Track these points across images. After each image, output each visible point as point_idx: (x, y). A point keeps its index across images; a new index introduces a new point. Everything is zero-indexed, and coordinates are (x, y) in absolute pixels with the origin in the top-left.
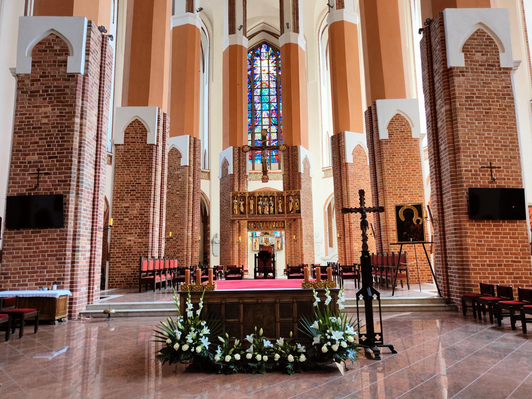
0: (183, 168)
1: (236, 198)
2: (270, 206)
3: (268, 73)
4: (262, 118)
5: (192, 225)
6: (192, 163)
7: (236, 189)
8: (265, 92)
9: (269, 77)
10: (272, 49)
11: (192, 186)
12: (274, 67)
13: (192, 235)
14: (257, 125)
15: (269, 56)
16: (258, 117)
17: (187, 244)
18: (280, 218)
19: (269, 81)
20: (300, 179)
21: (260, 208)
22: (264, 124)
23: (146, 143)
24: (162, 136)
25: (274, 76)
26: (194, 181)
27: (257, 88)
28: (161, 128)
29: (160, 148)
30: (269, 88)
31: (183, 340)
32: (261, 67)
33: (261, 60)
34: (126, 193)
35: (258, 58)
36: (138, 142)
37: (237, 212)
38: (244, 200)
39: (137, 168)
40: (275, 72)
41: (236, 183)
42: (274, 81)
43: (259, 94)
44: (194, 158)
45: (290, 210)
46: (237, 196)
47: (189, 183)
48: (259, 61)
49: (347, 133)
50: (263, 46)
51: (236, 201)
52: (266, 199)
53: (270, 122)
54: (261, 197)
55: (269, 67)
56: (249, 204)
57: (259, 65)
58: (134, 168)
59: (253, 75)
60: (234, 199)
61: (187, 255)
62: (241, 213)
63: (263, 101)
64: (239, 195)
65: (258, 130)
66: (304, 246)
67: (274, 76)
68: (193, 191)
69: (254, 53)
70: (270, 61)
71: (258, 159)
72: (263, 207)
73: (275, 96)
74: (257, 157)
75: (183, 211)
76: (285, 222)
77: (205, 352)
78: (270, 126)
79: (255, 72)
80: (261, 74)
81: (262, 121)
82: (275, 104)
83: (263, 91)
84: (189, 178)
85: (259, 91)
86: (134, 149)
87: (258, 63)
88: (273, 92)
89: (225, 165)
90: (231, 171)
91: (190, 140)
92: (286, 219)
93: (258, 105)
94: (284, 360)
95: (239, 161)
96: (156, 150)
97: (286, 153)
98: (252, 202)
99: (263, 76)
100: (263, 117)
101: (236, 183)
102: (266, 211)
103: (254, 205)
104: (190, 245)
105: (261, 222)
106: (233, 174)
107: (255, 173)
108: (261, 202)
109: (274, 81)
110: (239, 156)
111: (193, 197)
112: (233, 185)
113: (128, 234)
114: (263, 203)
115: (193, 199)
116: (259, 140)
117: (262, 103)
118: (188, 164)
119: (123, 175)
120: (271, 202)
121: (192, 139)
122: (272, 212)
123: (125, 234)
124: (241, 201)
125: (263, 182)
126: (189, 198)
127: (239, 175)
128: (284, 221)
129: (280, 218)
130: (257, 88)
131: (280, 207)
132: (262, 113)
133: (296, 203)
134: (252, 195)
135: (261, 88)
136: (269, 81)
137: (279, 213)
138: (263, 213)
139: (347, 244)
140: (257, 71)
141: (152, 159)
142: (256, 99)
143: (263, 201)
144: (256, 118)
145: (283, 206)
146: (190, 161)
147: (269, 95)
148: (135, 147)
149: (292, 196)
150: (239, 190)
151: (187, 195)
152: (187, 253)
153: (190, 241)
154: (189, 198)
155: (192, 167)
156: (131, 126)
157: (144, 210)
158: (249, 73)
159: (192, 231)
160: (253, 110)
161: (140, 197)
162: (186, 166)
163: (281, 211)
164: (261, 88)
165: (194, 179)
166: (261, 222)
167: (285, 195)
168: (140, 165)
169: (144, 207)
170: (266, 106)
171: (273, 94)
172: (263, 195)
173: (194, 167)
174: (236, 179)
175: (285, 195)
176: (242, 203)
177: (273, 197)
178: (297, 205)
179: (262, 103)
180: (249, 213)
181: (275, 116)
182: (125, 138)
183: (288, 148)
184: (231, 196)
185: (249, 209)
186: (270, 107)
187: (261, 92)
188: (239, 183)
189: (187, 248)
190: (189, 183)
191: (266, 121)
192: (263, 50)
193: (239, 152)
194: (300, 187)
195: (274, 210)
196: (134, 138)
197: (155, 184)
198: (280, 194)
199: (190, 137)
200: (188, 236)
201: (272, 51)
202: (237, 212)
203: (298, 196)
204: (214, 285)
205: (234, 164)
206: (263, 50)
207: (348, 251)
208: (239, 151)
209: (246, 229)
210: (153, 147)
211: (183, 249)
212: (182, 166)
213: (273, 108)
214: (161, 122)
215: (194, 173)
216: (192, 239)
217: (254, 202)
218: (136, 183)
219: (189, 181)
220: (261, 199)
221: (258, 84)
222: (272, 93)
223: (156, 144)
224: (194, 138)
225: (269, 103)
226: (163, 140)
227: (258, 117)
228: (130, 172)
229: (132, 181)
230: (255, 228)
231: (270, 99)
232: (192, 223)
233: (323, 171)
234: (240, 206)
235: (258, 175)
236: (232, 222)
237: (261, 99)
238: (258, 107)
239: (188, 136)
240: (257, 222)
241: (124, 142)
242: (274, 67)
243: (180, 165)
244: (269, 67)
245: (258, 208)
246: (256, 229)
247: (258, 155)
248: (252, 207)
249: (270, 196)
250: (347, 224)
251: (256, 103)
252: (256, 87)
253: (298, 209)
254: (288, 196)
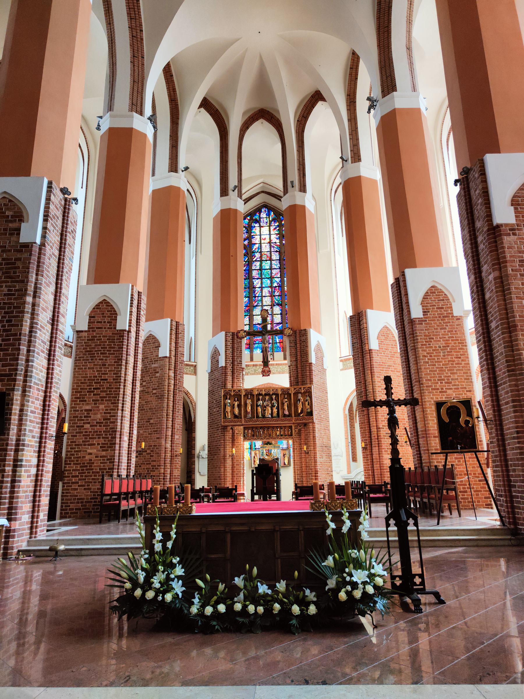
0: (161, 360)
1: (228, 397)
2: (273, 406)
3: (270, 243)
4: (262, 297)
5: (172, 434)
6: (173, 353)
7: (229, 386)
8: (266, 265)
9: (270, 246)
10: (274, 214)
11: (173, 382)
12: (277, 234)
13: (171, 446)
14: (257, 306)
15: (270, 222)
16: (257, 295)
17: (165, 458)
18: (287, 423)
19: (271, 252)
20: (311, 371)
21: (260, 409)
22: (264, 304)
23: (115, 328)
24: (135, 319)
25: (277, 246)
26: (175, 376)
27: (256, 261)
28: (135, 310)
29: (133, 334)
30: (271, 260)
31: (147, 585)
32: (260, 235)
33: (260, 227)
34: (88, 392)
35: (257, 225)
36: (105, 328)
37: (229, 416)
38: (239, 400)
39: (103, 360)
40: (278, 241)
41: (229, 378)
42: (277, 251)
43: (258, 268)
44: (176, 348)
45: (299, 412)
46: (230, 395)
47: (169, 379)
48: (258, 228)
49: (369, 312)
50: (263, 210)
51: (229, 401)
52: (267, 398)
53: (272, 301)
54: (261, 395)
55: (270, 234)
56: (246, 404)
57: (258, 233)
58: (99, 359)
59: (251, 244)
60: (227, 399)
61: (164, 474)
62: (236, 416)
63: (263, 277)
64: (232, 394)
65: (257, 311)
66: (319, 460)
67: (277, 246)
68: (174, 389)
69: (251, 219)
70: (272, 228)
71: (257, 347)
72: (264, 408)
73: (279, 270)
74: (256, 345)
75: (160, 415)
76: (293, 428)
77: (177, 601)
78: (272, 306)
79: (254, 241)
80: (261, 243)
81: (262, 301)
82: (278, 280)
83: (264, 263)
84: (169, 373)
85: (258, 264)
86: (100, 337)
87: (256, 230)
88: (276, 265)
89: (215, 355)
90: (222, 363)
91: (171, 325)
92: (293, 424)
93: (257, 281)
94: (286, 611)
95: (233, 350)
96: (128, 337)
97: (292, 338)
98: (249, 402)
99: (263, 245)
100: (264, 295)
101: (229, 378)
103: (252, 406)
104: (168, 461)
105: (261, 428)
106: (225, 367)
107: (254, 365)
109: (277, 251)
110: (233, 343)
111: (174, 397)
112: (226, 380)
113: (88, 445)
114: (263, 403)
115: (174, 399)
116: (258, 324)
117: (261, 279)
118: (168, 355)
119: (85, 369)
120: (274, 401)
121: (174, 323)
122: (275, 414)
123: (85, 445)
124: (235, 401)
125: (263, 376)
126: (168, 398)
127: (232, 367)
128: (291, 427)
129: (287, 423)
130: (256, 261)
131: (286, 407)
132: (262, 290)
133: (307, 403)
134: (249, 393)
135: (261, 261)
136: (271, 252)
137: (285, 416)
138: (264, 416)
139: (376, 455)
140: (256, 240)
141: (122, 348)
142: (255, 274)
143: (264, 400)
144: (255, 297)
145: (289, 407)
146: (170, 351)
147: (271, 269)
148: (102, 334)
149: (301, 393)
150: (232, 387)
151: (166, 395)
152: (164, 471)
153: (169, 455)
154: (168, 398)
155: (173, 358)
156: (97, 308)
157: (110, 413)
158: (246, 242)
159: (172, 441)
160: (251, 288)
161: (106, 397)
162: (166, 357)
163: (287, 413)
164: (261, 261)
165: (175, 373)
166: (261, 428)
167: (292, 392)
168: (107, 357)
169: (110, 410)
170: (267, 282)
171: (276, 267)
172: (264, 393)
173: (175, 359)
174: (229, 373)
175: (292, 392)
176: (236, 403)
177: (277, 395)
178: (308, 405)
179: (261, 279)
180: (245, 416)
181: (278, 294)
182: (89, 323)
183: (295, 332)
184: (223, 394)
185: (246, 411)
186: (272, 283)
187: (261, 265)
188: (232, 378)
189: (165, 463)
190: (169, 379)
191: (267, 301)
192: (263, 215)
193: (233, 339)
194: (311, 382)
195: (278, 411)
196: (101, 322)
197: (125, 380)
198: (285, 392)
199: (172, 321)
200: (166, 448)
201: (274, 216)
202: (229, 416)
203: (308, 393)
204: (191, 507)
205: (226, 354)
206: (263, 215)
207: (376, 466)
208: (233, 337)
209: (242, 438)
210: (123, 333)
211: (160, 466)
212: (160, 358)
213: (275, 285)
214: (135, 302)
215: (175, 366)
216: (171, 451)
217: (253, 401)
218: (101, 380)
219: (169, 376)
220: (261, 397)
221: (258, 255)
222: (274, 266)
223: (127, 329)
224: (177, 322)
225: (271, 278)
226: (137, 325)
227: (257, 295)
228: (94, 365)
229: (96, 377)
230: (253, 436)
231: (271, 273)
232: (172, 431)
233: (341, 361)
234: (234, 408)
235: (258, 367)
236: (224, 429)
237: (261, 273)
238: (257, 283)
239: (169, 320)
240: (256, 428)
241: (89, 328)
242: (277, 234)
243: (158, 356)
244: (270, 234)
245: (257, 409)
246: (255, 437)
247: (257, 342)
248: (249, 409)
249: (273, 394)
250: (374, 429)
251: (254, 279)
252: (254, 260)
253: (309, 410)
254: (296, 394)
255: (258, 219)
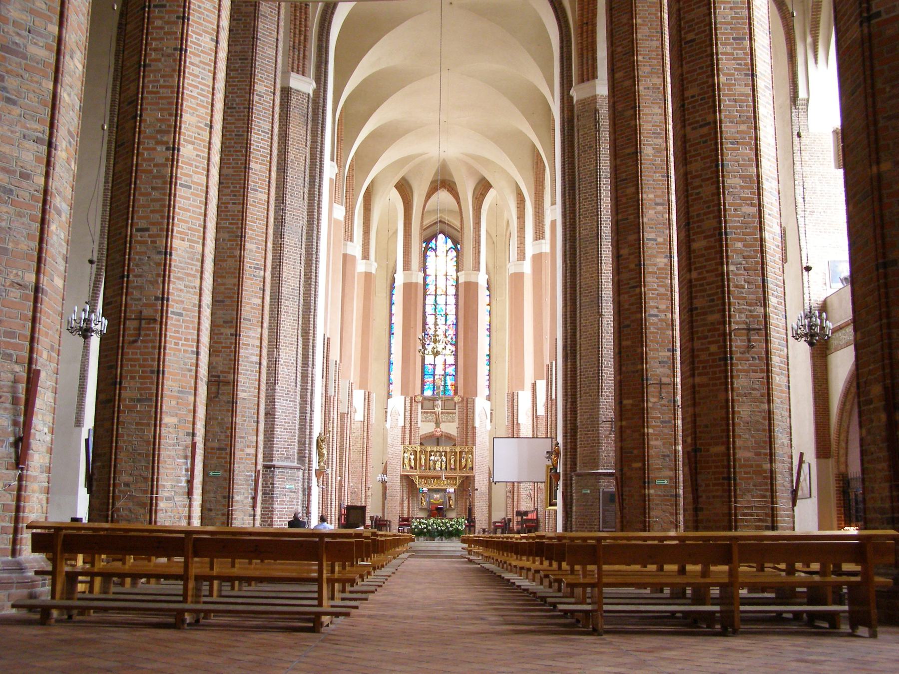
2: (442, 461)
8: (441, 300)
15: (447, 251)
20: (474, 433)
29: (349, 416)
37: (408, 468)
49: (520, 393)
52: (438, 454)
54: (433, 451)
56: (420, 458)
60: (404, 452)
62: (411, 468)
69: (427, 245)
72: (435, 462)
79: (428, 272)
88: (452, 300)
95: (411, 412)
98: (423, 457)
102: (438, 468)
105: (432, 478)
108: (432, 458)
120: (443, 458)
121: (367, 394)
122: (444, 467)
131: (452, 461)
137: (451, 469)
138: (435, 469)
142: (429, 309)
163: (453, 467)
164: (436, 295)
166: (432, 478)
170: (441, 320)
176: (412, 457)
177: (446, 452)
185: (421, 465)
194: (474, 444)
220: (433, 454)
221: (431, 289)
240: (429, 478)
248: (423, 461)
255: (434, 248)
